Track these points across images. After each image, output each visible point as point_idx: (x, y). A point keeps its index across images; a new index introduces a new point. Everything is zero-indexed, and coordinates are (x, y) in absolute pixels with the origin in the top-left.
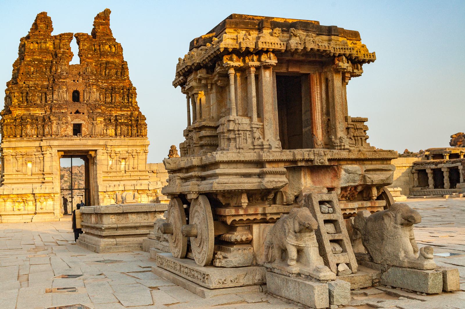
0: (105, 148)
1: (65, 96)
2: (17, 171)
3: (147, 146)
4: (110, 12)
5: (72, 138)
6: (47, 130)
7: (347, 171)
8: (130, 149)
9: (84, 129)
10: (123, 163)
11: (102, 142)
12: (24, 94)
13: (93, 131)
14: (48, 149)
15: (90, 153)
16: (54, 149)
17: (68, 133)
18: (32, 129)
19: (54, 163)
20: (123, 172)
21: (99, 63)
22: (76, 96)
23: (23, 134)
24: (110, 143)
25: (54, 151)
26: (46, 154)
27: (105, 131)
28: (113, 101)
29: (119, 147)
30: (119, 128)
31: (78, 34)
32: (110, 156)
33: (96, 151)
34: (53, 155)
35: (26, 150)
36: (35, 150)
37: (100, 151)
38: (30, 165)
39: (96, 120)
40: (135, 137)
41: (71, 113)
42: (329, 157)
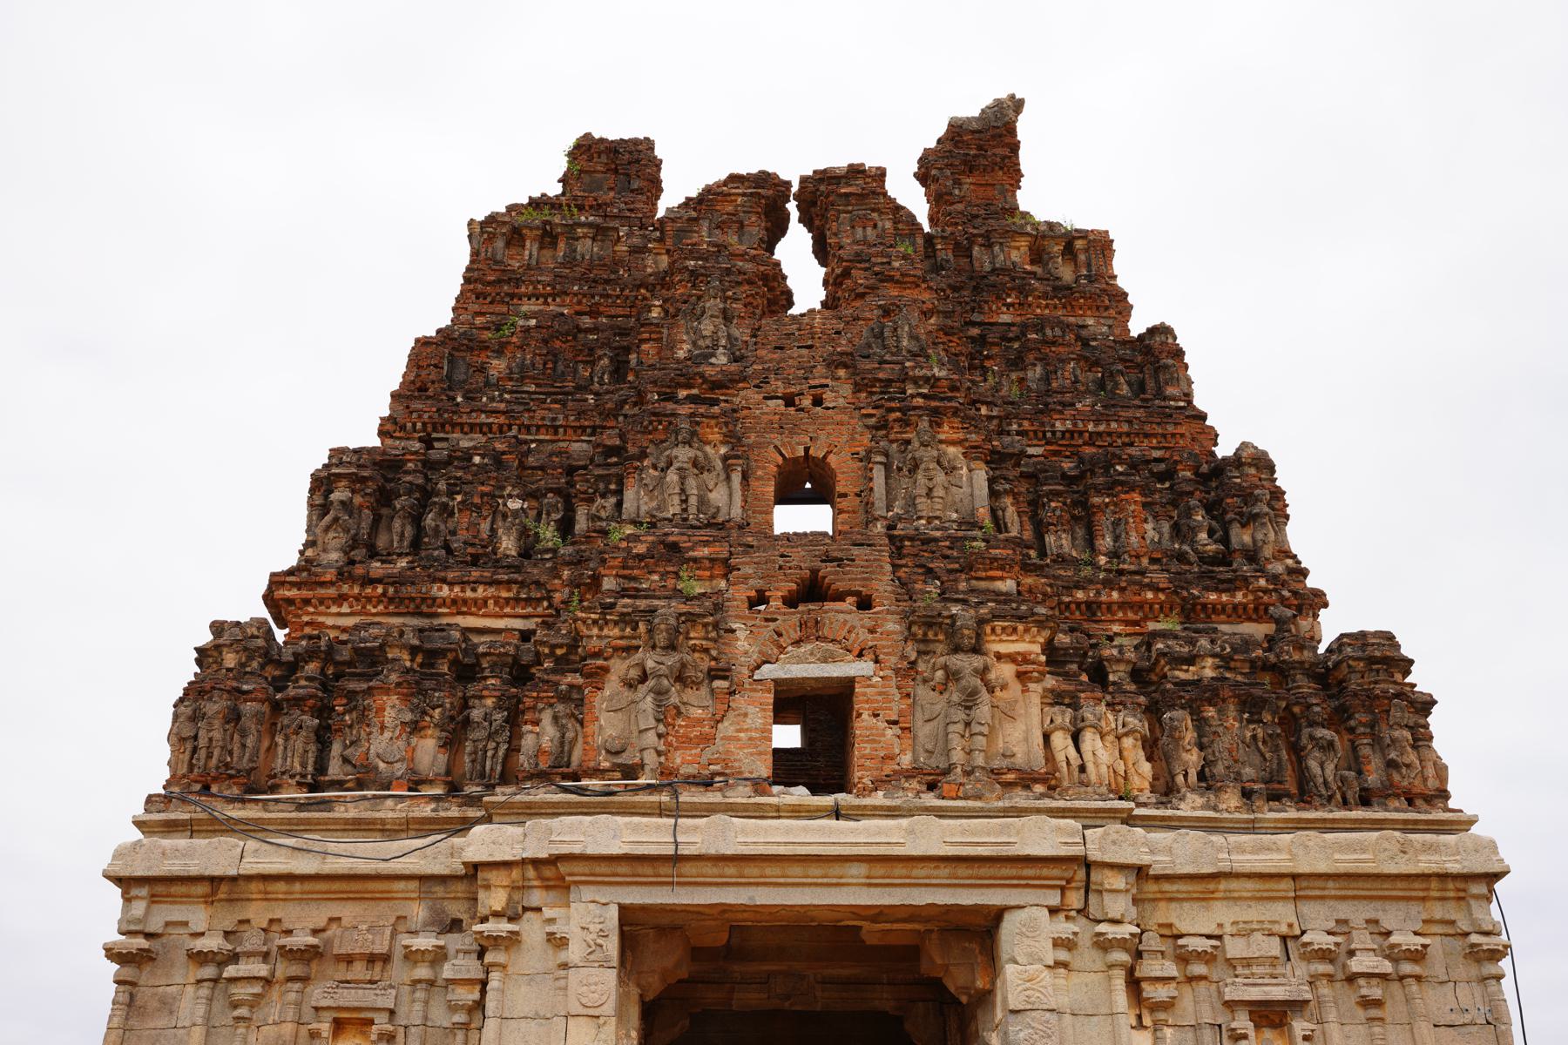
1: (718, 496)
3: (1478, 889)
4: (1017, 105)
6: (541, 735)
9: (864, 724)
11: (1043, 836)
13: (956, 742)
14: (536, 897)
16: (588, 893)
18: (415, 728)
23: (335, 770)
25: (590, 918)
27: (1061, 741)
29: (1205, 899)
34: (575, 953)
35: (335, 909)
36: (418, 912)
39: (977, 650)
40: (1345, 804)
41: (761, 598)
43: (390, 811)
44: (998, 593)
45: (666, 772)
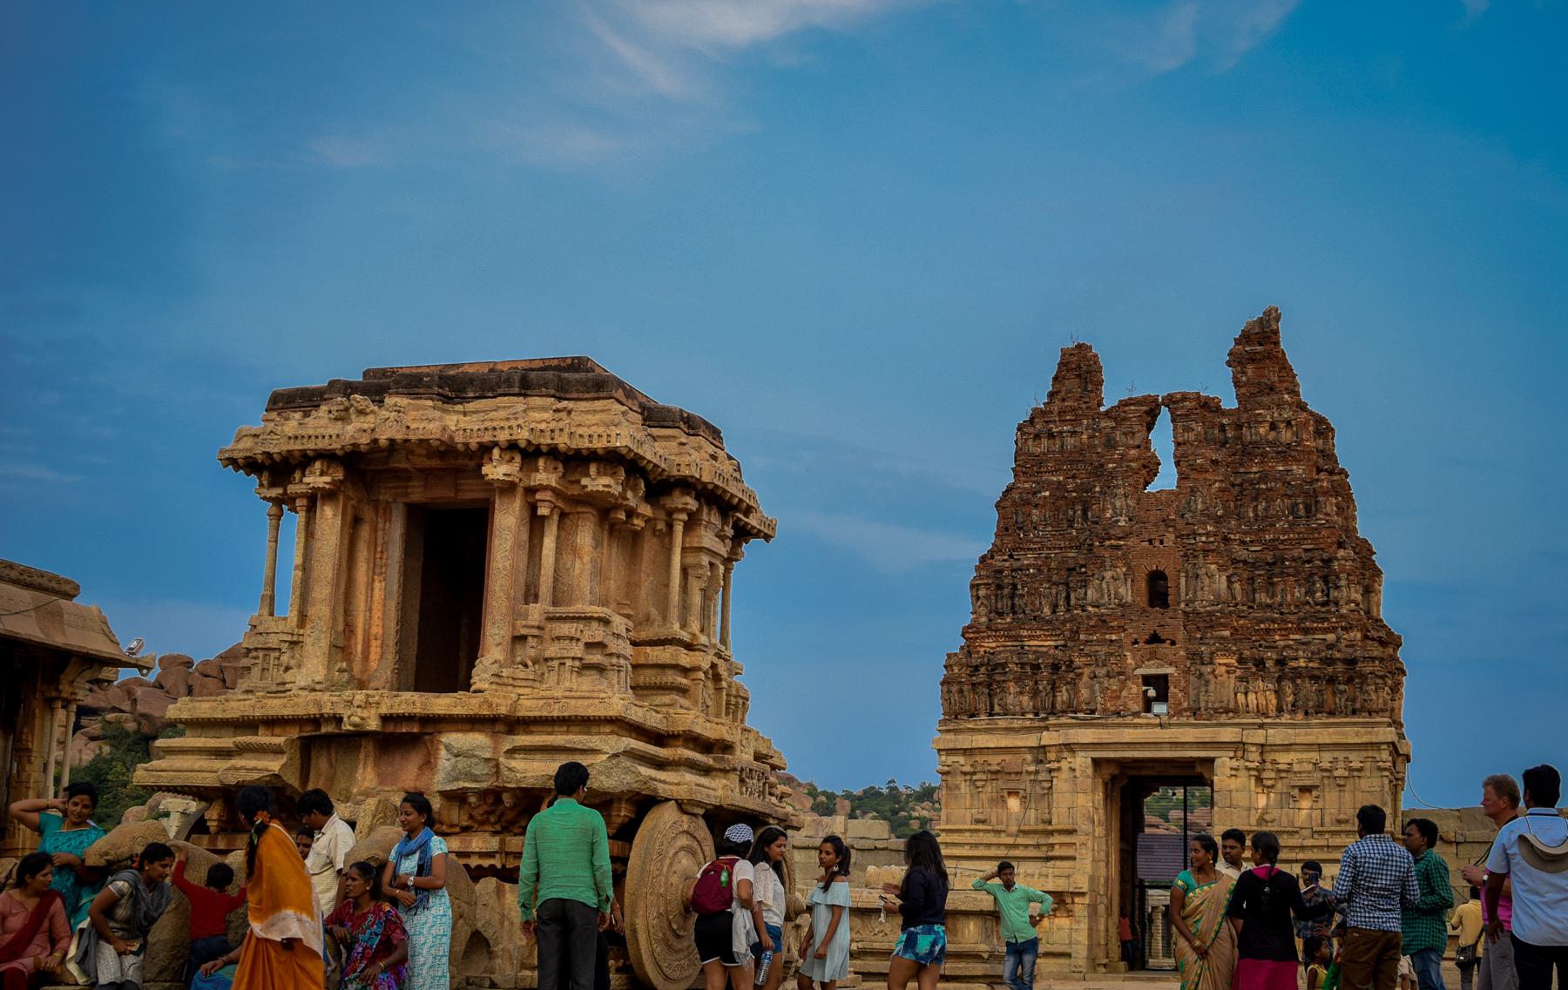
0: (1240, 754)
1: (1122, 591)
2: (978, 821)
4: (1278, 319)
5: (1136, 721)
6: (1063, 696)
7: (448, 748)
8: (1326, 758)
10: (1306, 803)
11: (1228, 734)
12: (1006, 591)
14: (1066, 754)
15: (1199, 769)
16: (1081, 754)
17: (1125, 705)
18: (1021, 693)
19: (1079, 800)
20: (1306, 833)
21: (1239, 481)
22: (1158, 590)
23: (997, 709)
24: (1258, 736)
25: (1082, 761)
26: (1059, 769)
27: (1241, 697)
28: (1279, 599)
30: (1288, 688)
31: (1170, 396)
32: (1259, 780)
33: (1211, 761)
34: (1078, 773)
36: (1029, 757)
37: (1224, 763)
38: (1014, 804)
40: (1346, 716)
42: (384, 710)
43: (1017, 724)
44: (1223, 638)
45: (1105, 710)
